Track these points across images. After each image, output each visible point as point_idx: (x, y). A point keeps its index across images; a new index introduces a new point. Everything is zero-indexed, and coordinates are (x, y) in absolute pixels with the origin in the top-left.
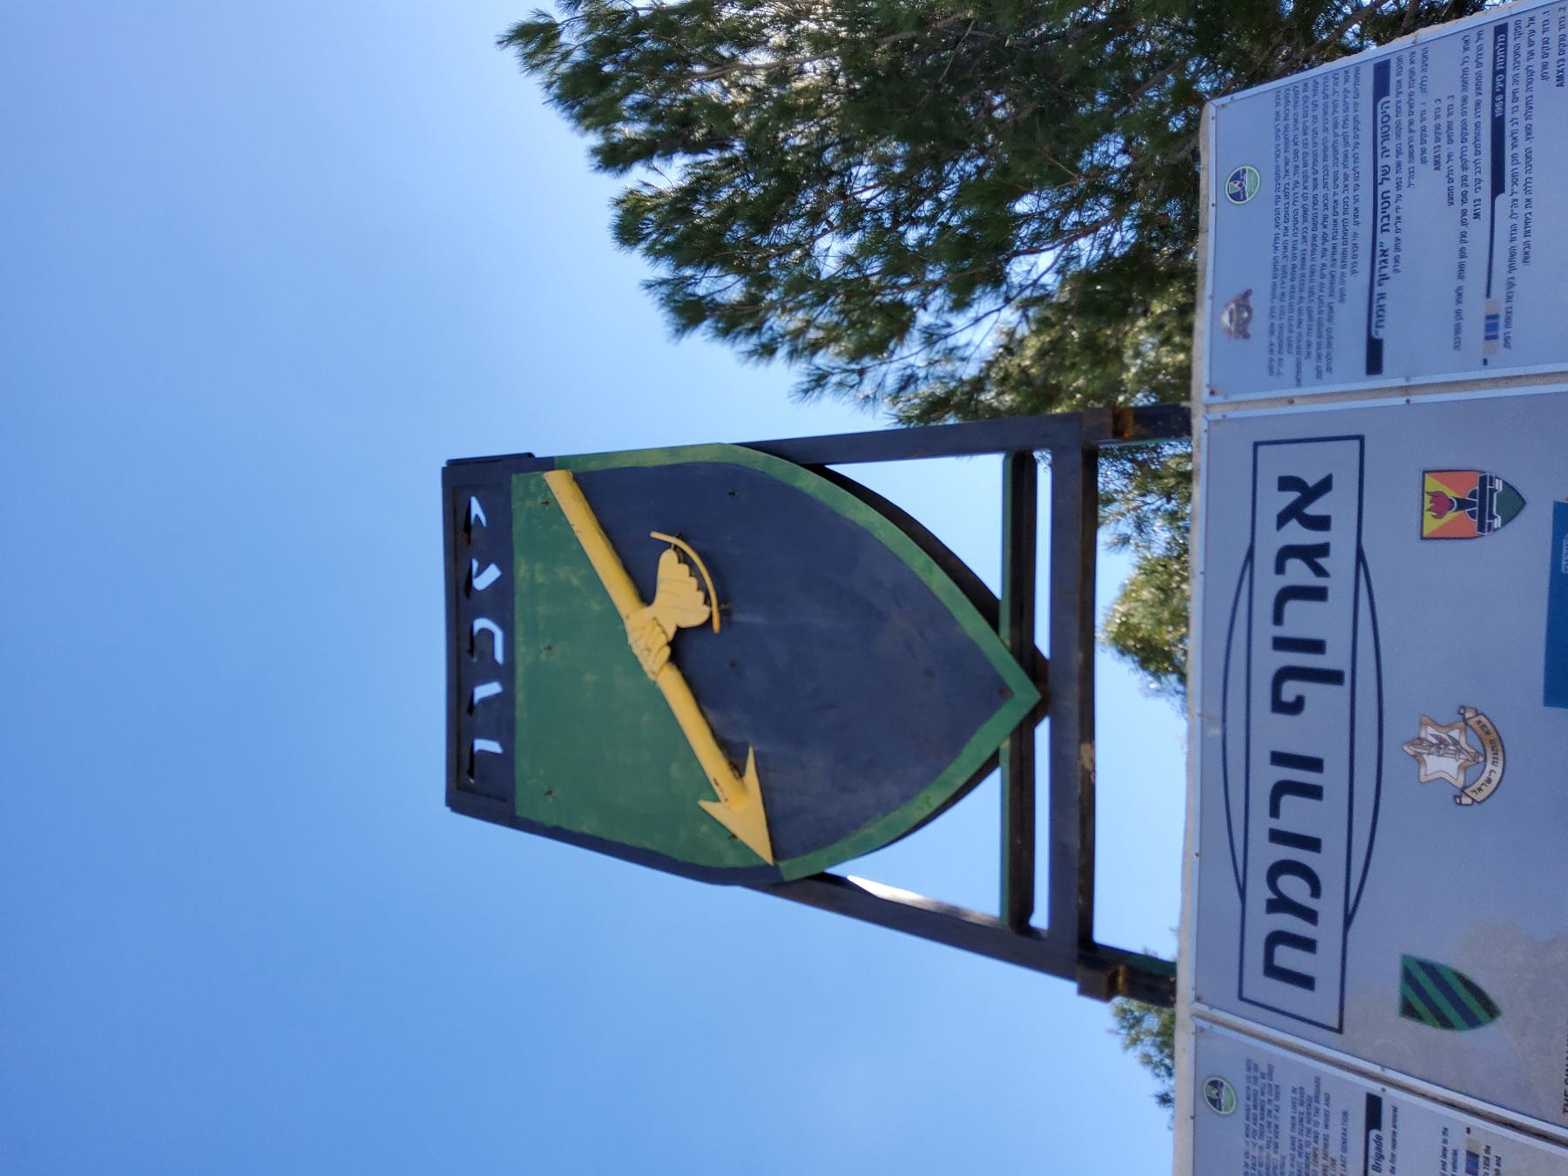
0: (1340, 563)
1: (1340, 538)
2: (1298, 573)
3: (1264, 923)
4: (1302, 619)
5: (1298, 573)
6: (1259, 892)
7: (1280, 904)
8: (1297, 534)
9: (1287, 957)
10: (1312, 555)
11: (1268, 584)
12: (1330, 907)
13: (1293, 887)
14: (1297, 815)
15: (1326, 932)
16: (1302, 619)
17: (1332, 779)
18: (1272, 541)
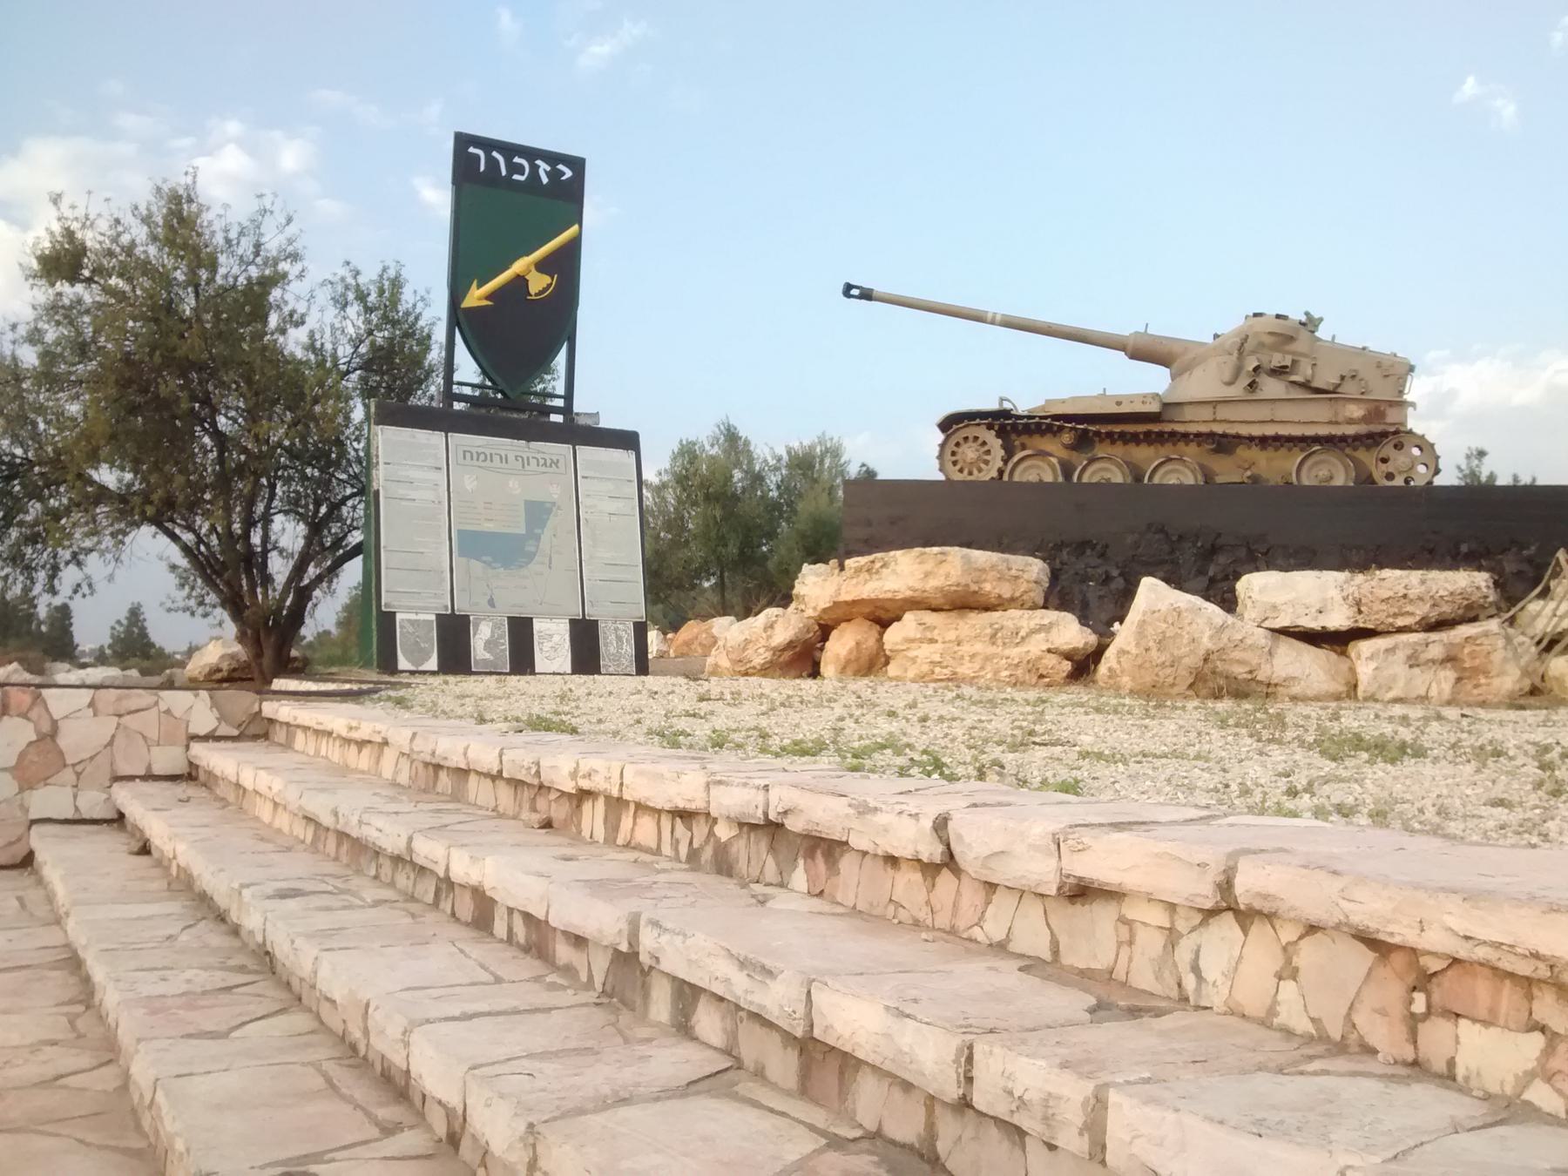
0: (544, 469)
3: (474, 450)
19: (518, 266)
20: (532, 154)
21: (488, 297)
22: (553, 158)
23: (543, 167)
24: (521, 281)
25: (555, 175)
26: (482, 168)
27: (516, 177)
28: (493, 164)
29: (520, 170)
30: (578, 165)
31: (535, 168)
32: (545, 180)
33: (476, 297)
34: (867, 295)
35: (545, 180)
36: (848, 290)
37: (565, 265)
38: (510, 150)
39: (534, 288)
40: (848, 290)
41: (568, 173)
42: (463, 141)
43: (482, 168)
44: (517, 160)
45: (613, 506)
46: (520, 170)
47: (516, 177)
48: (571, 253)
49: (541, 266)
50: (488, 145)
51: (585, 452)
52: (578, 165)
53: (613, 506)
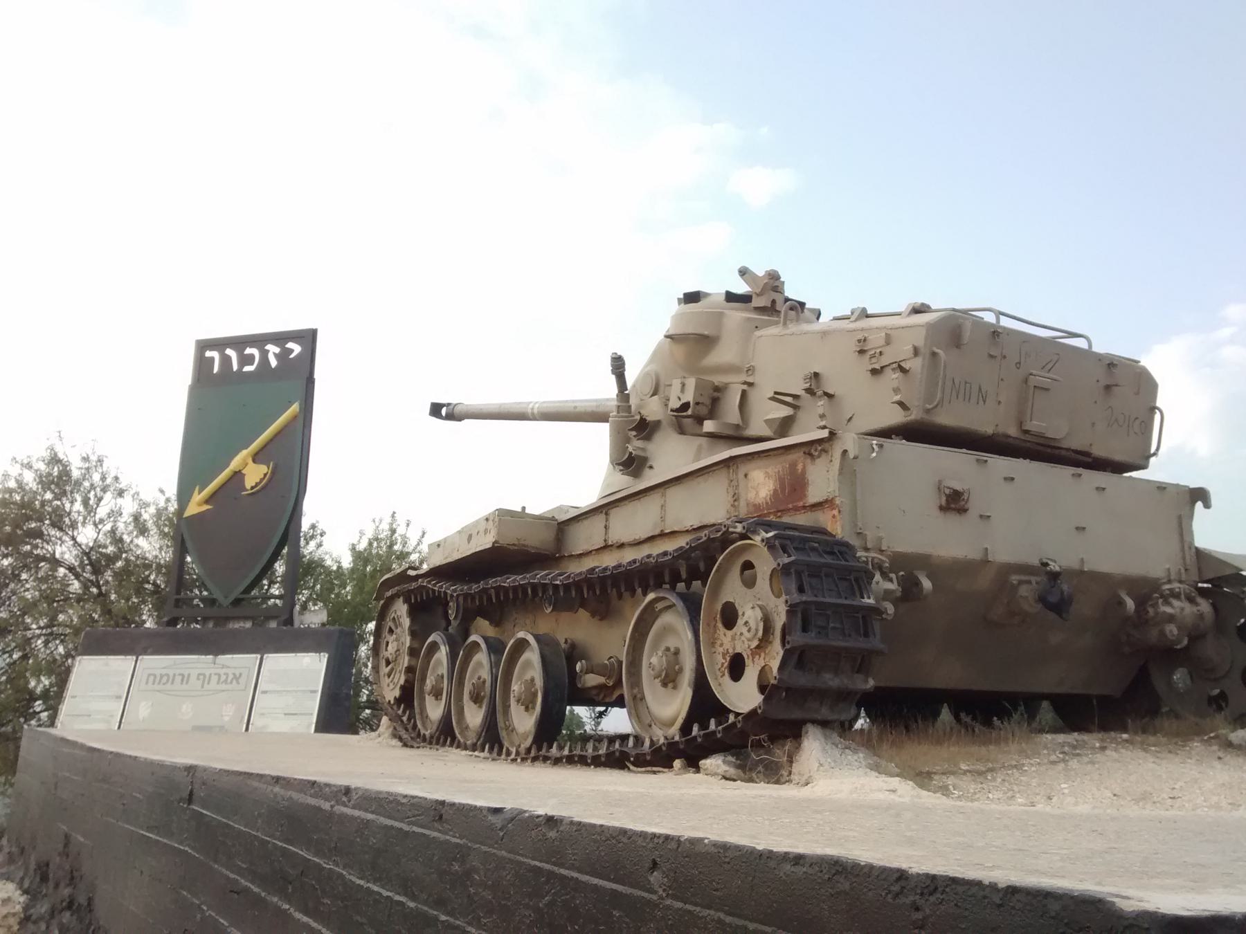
0: (224, 687)
1: (229, 687)
2: (223, 678)
4: (214, 679)
5: (223, 678)
6: (164, 672)
7: (162, 676)
8: (231, 677)
9: (152, 678)
10: (226, 681)
11: (222, 671)
12: (161, 687)
13: (165, 679)
14: (178, 679)
15: (156, 687)
16: (214, 679)
17: (184, 686)
18: (230, 672)
19: (235, 464)
20: (259, 341)
21: (207, 502)
22: (280, 338)
23: (273, 349)
24: (238, 475)
25: (283, 355)
26: (216, 369)
27: (247, 369)
28: (226, 360)
29: (250, 360)
30: (308, 338)
31: (264, 354)
32: (274, 363)
34: (454, 415)
35: (274, 363)
36: (436, 410)
38: (239, 343)
39: (250, 481)
40: (436, 410)
41: (296, 348)
43: (216, 369)
44: (248, 351)
46: (250, 360)
47: (247, 369)
50: (220, 344)
52: (308, 338)
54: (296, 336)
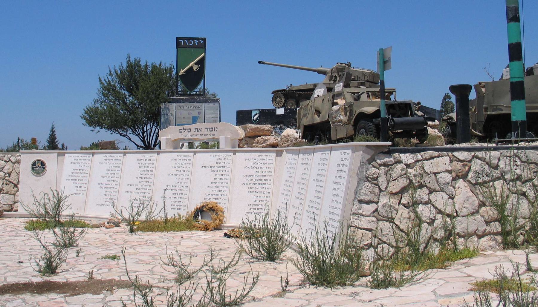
19: (191, 64)
20: (193, 39)
24: (192, 68)
25: (199, 43)
28: (185, 43)
33: (182, 72)
37: (201, 63)
39: (195, 69)
40: (260, 62)
41: (202, 42)
42: (178, 39)
45: (213, 116)
46: (191, 43)
48: (203, 59)
49: (196, 64)
50: (183, 39)
51: (206, 104)
52: (204, 40)
53: (213, 116)
54: (202, 39)
